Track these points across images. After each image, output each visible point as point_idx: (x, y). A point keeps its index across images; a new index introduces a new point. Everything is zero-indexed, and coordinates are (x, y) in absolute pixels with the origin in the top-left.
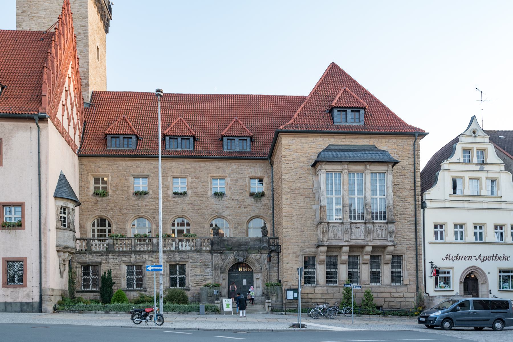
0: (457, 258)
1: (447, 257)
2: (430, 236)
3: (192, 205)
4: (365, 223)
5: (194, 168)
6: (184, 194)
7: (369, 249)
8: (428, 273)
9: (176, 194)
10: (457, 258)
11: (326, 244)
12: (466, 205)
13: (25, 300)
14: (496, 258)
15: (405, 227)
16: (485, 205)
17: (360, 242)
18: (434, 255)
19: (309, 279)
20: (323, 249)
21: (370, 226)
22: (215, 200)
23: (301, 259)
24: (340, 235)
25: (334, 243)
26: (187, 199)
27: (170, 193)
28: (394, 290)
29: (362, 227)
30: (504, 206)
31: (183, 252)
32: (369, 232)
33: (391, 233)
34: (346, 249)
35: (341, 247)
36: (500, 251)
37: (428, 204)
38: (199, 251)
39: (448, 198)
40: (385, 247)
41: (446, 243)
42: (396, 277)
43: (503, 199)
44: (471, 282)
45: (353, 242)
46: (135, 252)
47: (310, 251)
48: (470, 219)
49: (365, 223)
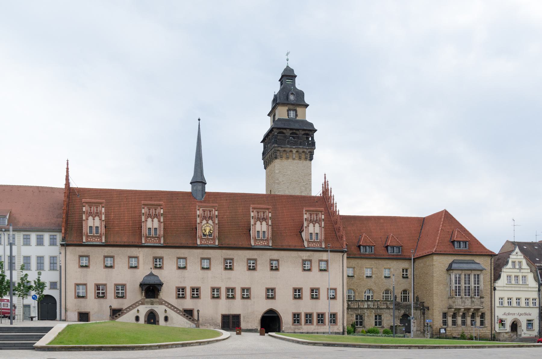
0: (509, 314)
1: (505, 314)
2: (497, 304)
3: (375, 283)
4: (471, 298)
5: (376, 264)
6: (370, 277)
7: (472, 310)
8: (496, 321)
9: (367, 277)
10: (509, 314)
11: (454, 307)
12: (513, 289)
13: (337, 331)
14: (526, 314)
15: (487, 300)
16: (521, 289)
17: (469, 307)
18: (499, 313)
19: (445, 323)
20: (453, 310)
21: (473, 299)
22: (385, 280)
23: (442, 314)
24: (460, 303)
25: (458, 307)
26: (373, 280)
27: (365, 277)
28: (481, 329)
29: (470, 300)
30: (530, 289)
31: (381, 309)
32: (472, 302)
33: (482, 303)
34: (463, 310)
35: (460, 309)
36: (528, 311)
37: (497, 288)
38: (388, 308)
39: (505, 285)
40: (478, 309)
41: (504, 307)
42: (482, 323)
43: (529, 286)
44: (514, 326)
45: (466, 307)
46: (361, 308)
47: (445, 310)
48: (514, 295)
49: (471, 298)
